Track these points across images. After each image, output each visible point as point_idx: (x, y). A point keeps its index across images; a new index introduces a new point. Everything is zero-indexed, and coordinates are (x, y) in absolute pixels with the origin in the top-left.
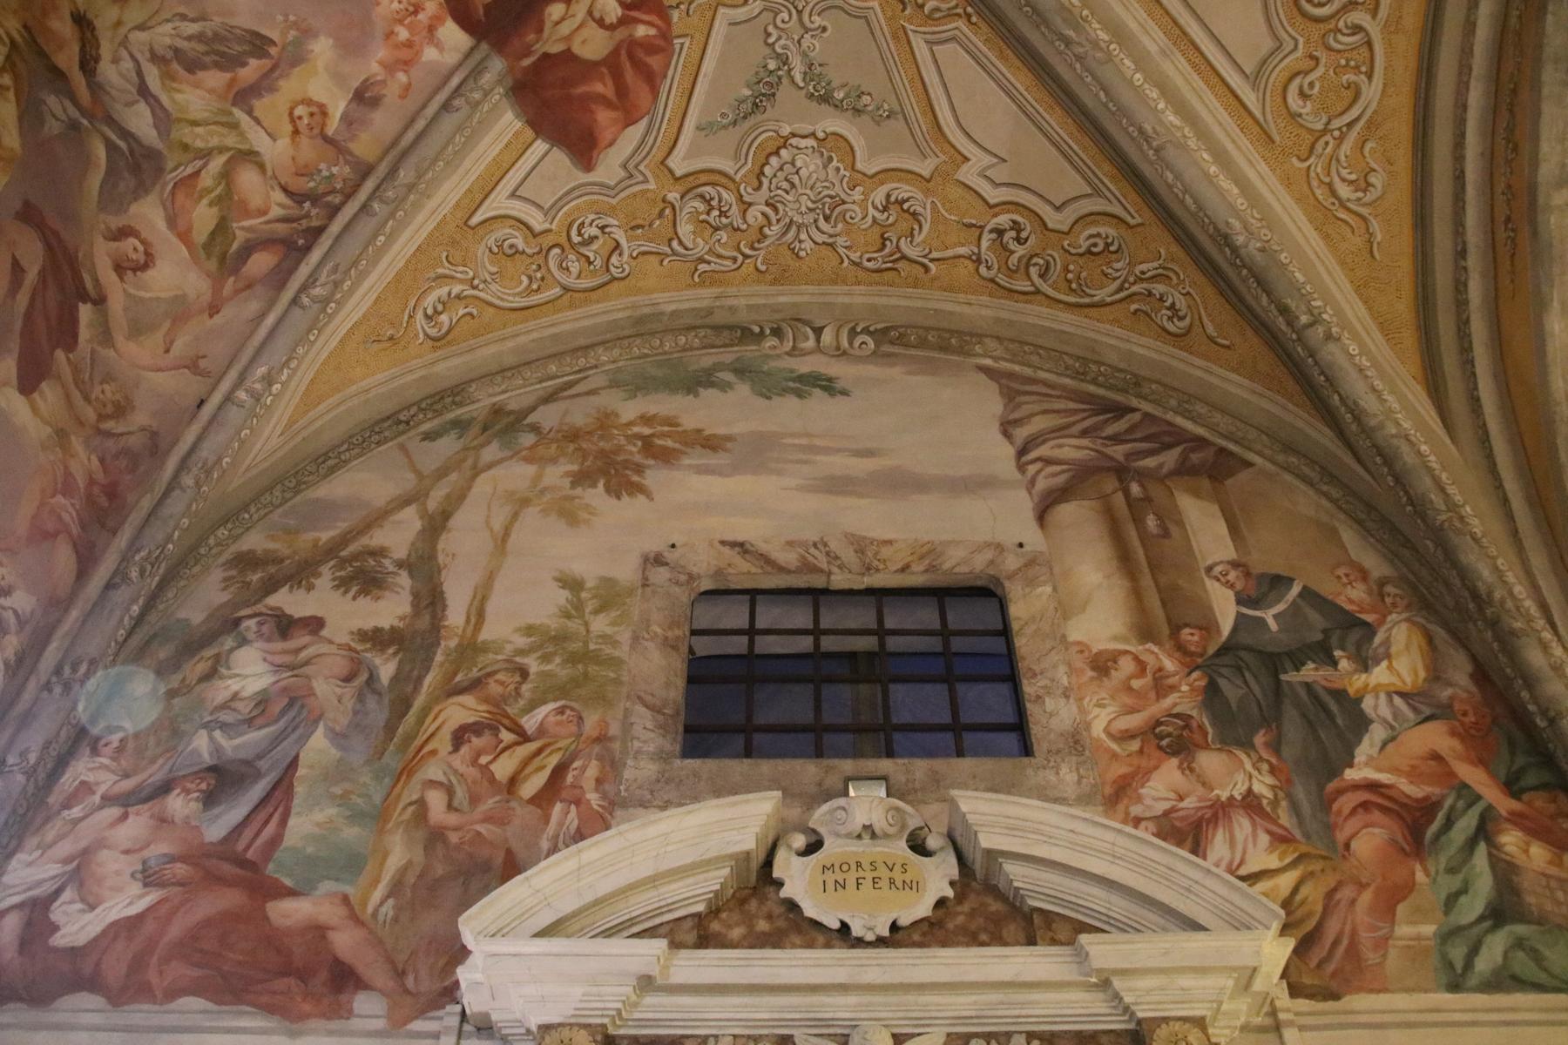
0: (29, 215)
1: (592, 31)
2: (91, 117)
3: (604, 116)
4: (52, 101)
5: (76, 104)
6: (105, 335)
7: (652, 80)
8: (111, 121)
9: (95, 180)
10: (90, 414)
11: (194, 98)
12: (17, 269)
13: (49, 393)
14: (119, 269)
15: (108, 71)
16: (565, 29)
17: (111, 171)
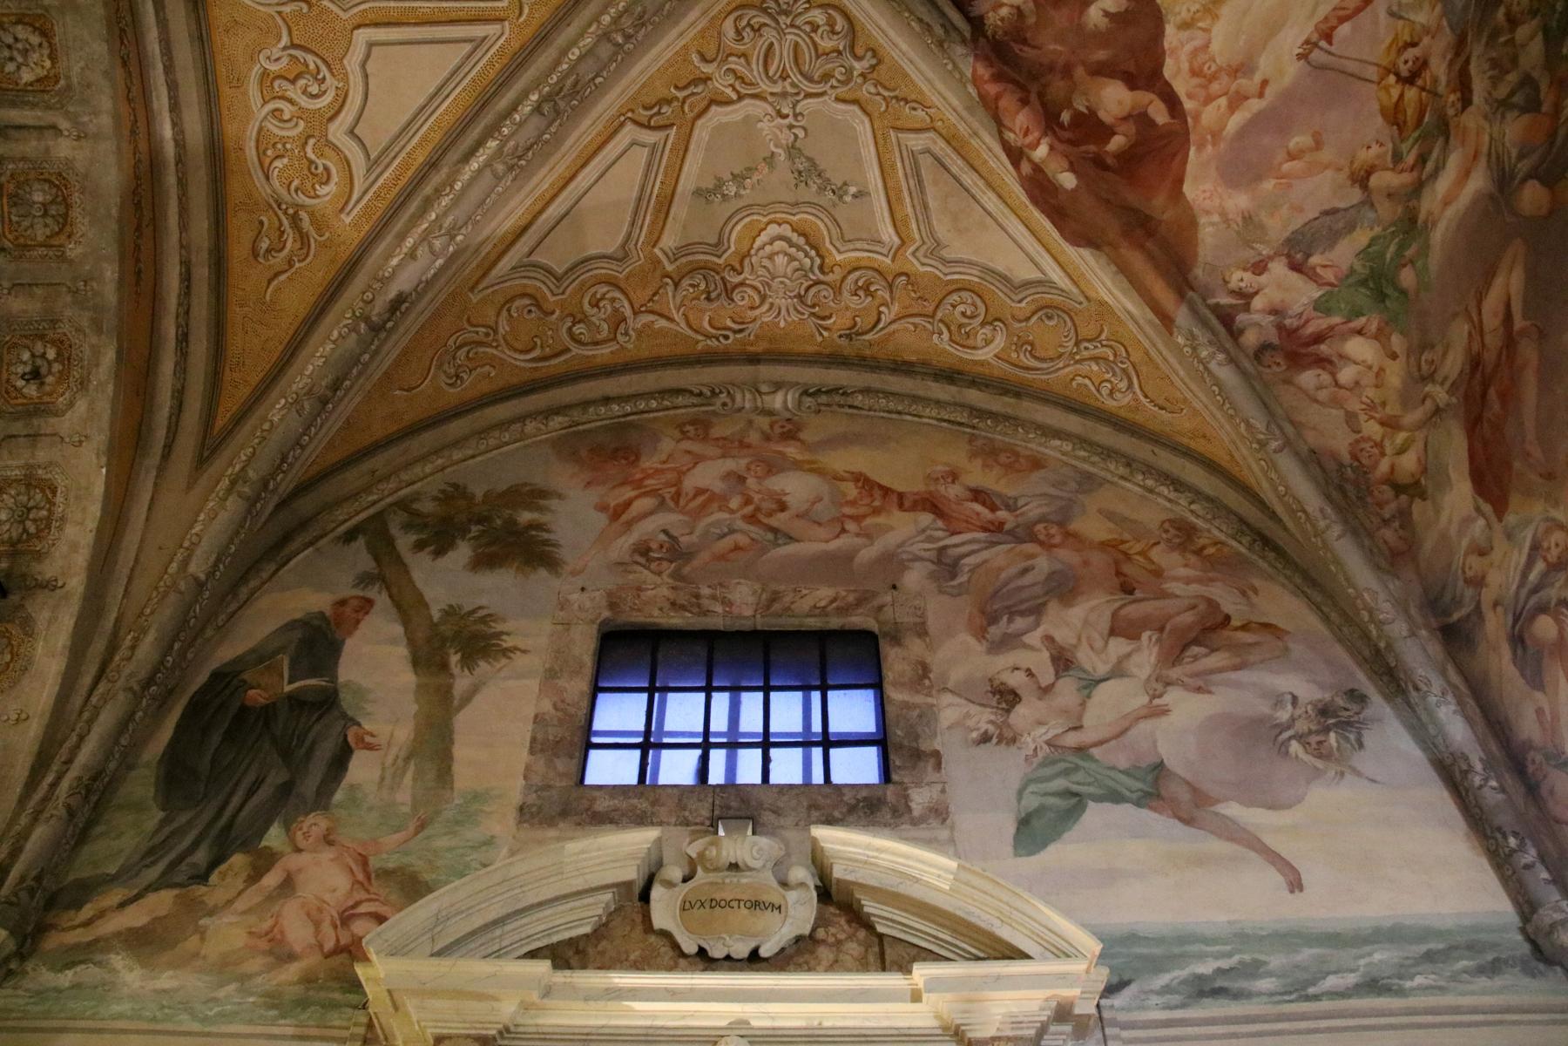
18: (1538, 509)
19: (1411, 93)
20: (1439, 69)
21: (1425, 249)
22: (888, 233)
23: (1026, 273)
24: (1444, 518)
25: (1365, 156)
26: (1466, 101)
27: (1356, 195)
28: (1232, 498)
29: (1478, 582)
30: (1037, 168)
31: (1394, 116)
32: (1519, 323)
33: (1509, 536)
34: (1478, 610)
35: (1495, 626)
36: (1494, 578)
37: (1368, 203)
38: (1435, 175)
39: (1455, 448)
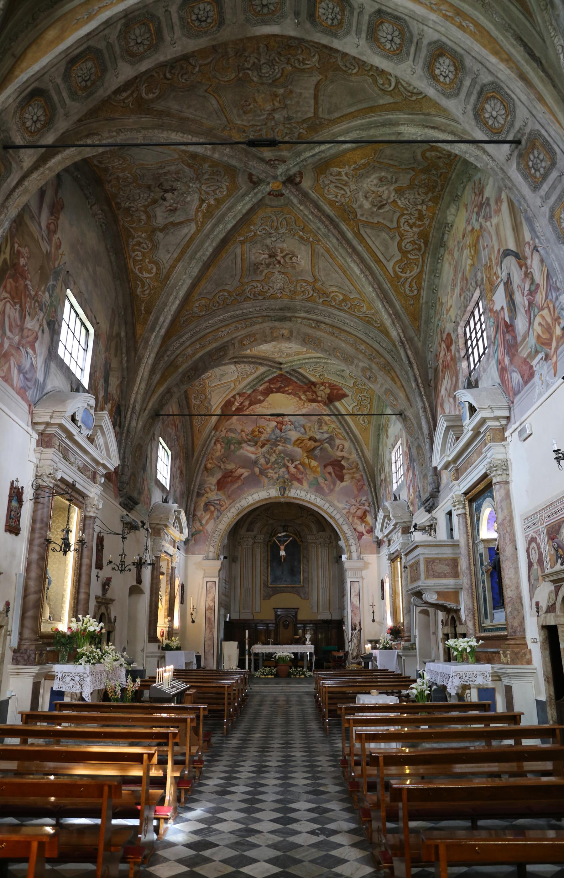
0: (325, 466)
1: (326, 391)
2: (322, 444)
3: (340, 392)
4: (316, 452)
5: (318, 447)
6: (348, 459)
7: (335, 385)
8: (324, 440)
9: (329, 449)
10: (355, 469)
11: (325, 428)
12: (330, 473)
13: (347, 477)
14: (342, 451)
15: (318, 437)
16: (323, 395)
17: (330, 444)
18: (223, 497)
19: (257, 433)
20: (263, 437)
21: (238, 449)
22: (213, 385)
23: (212, 403)
24: (208, 479)
25: (245, 429)
26: (262, 447)
27: (239, 431)
28: (190, 447)
29: (207, 493)
30: (233, 403)
31: (253, 431)
32: (242, 478)
33: (217, 494)
34: (203, 495)
35: (204, 499)
36: (209, 495)
37: (239, 434)
38: (249, 445)
39: (219, 475)
